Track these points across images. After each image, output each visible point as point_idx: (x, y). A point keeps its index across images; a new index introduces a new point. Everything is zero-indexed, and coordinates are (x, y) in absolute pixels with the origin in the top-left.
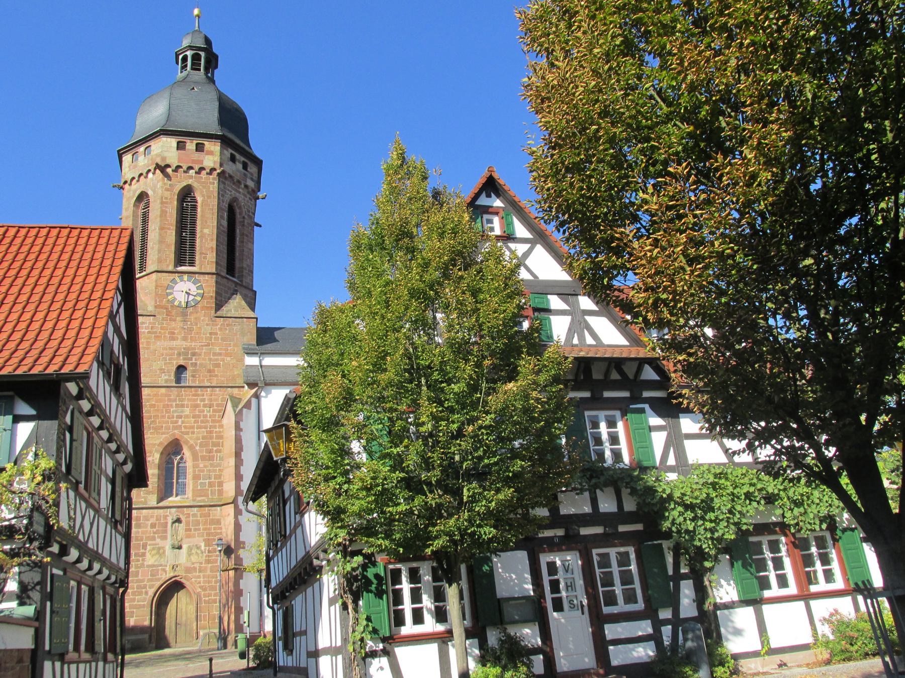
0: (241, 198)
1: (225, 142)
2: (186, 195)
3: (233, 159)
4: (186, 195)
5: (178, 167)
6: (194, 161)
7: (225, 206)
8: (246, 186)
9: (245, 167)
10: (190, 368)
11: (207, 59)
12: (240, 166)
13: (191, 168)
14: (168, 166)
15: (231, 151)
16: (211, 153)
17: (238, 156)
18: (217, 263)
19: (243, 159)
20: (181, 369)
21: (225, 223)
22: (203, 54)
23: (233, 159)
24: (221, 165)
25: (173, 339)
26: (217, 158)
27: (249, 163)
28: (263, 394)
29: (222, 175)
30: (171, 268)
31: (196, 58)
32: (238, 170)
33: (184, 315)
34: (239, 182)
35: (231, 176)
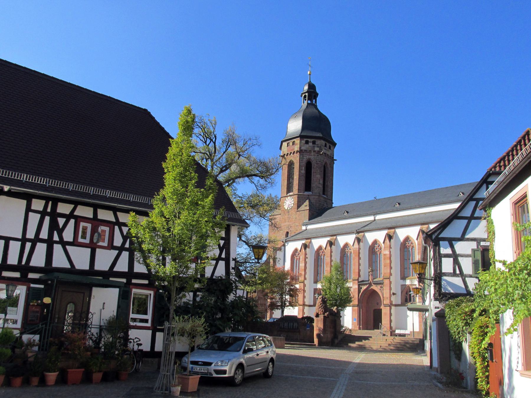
0: (312, 157)
1: (301, 137)
2: (291, 165)
3: (307, 142)
4: (291, 165)
5: (288, 154)
6: (292, 150)
7: (304, 164)
8: (314, 151)
9: (314, 143)
10: (289, 232)
11: (312, 94)
12: (311, 144)
13: (291, 153)
14: (285, 155)
15: (305, 140)
16: (297, 144)
17: (309, 140)
18: (298, 189)
19: (312, 140)
20: (287, 233)
21: (303, 172)
22: (307, 94)
23: (307, 142)
24: (300, 148)
25: (285, 222)
26: (299, 146)
27: (316, 140)
28: (286, 244)
29: (301, 151)
30: (285, 195)
31: (305, 97)
32: (310, 146)
33: (288, 212)
34: (310, 151)
35: (305, 151)
